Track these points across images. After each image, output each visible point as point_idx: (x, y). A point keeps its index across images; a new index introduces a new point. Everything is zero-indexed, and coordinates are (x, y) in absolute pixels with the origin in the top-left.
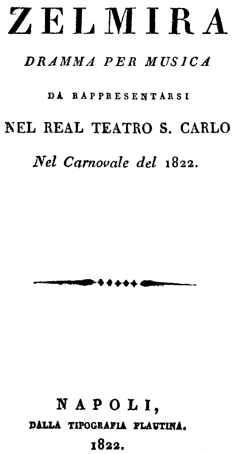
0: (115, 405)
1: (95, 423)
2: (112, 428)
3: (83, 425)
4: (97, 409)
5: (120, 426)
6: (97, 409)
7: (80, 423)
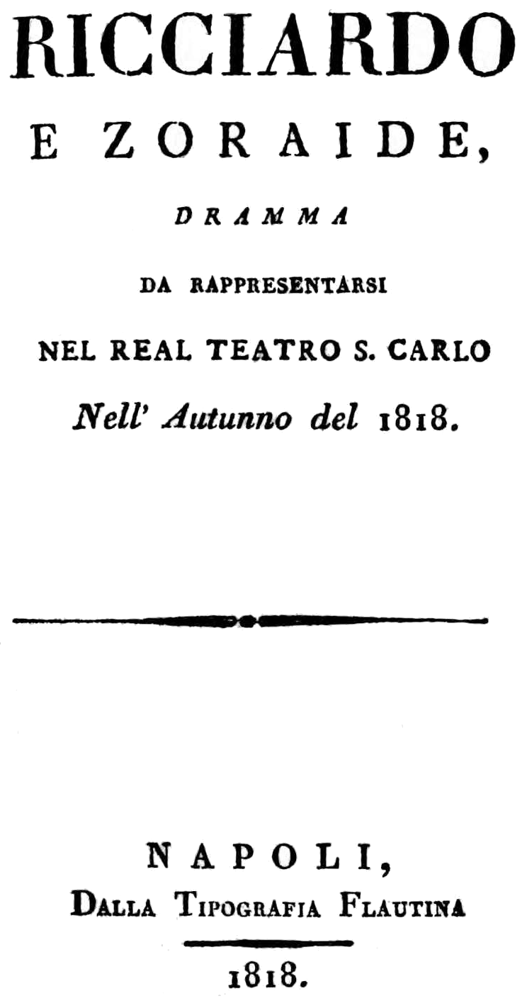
0: (285, 856)
1: (247, 904)
2: (287, 915)
3: (217, 908)
4: (290, 916)
5: (306, 911)
6: (290, 916)
7: (211, 903)
